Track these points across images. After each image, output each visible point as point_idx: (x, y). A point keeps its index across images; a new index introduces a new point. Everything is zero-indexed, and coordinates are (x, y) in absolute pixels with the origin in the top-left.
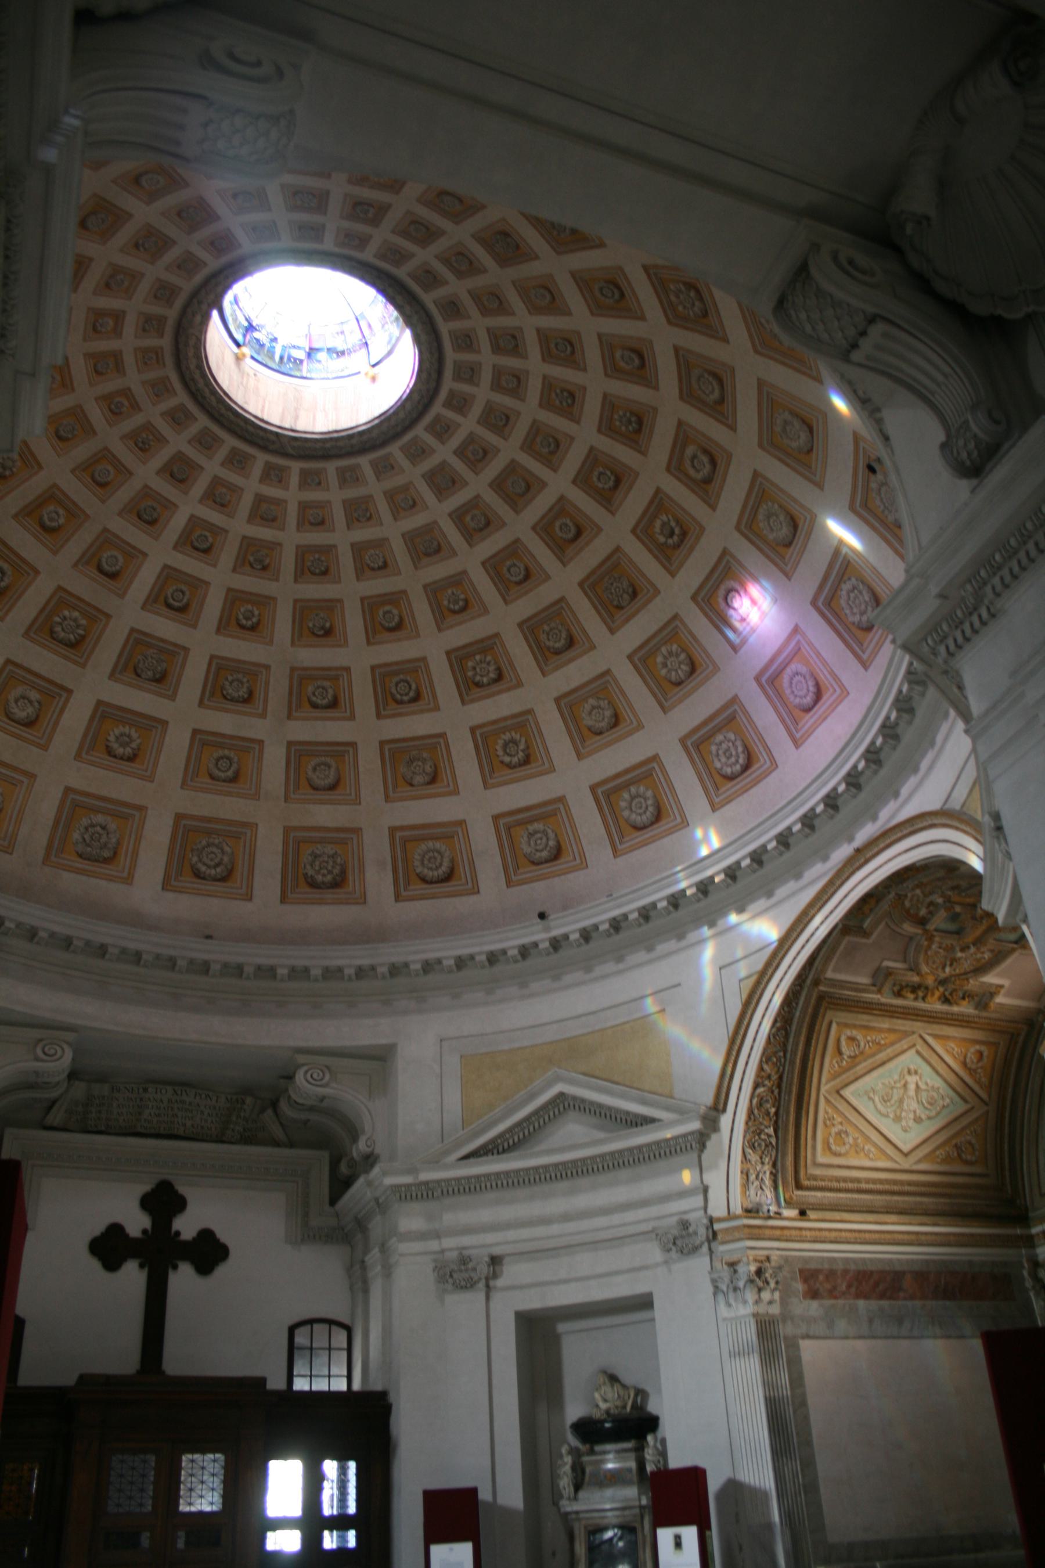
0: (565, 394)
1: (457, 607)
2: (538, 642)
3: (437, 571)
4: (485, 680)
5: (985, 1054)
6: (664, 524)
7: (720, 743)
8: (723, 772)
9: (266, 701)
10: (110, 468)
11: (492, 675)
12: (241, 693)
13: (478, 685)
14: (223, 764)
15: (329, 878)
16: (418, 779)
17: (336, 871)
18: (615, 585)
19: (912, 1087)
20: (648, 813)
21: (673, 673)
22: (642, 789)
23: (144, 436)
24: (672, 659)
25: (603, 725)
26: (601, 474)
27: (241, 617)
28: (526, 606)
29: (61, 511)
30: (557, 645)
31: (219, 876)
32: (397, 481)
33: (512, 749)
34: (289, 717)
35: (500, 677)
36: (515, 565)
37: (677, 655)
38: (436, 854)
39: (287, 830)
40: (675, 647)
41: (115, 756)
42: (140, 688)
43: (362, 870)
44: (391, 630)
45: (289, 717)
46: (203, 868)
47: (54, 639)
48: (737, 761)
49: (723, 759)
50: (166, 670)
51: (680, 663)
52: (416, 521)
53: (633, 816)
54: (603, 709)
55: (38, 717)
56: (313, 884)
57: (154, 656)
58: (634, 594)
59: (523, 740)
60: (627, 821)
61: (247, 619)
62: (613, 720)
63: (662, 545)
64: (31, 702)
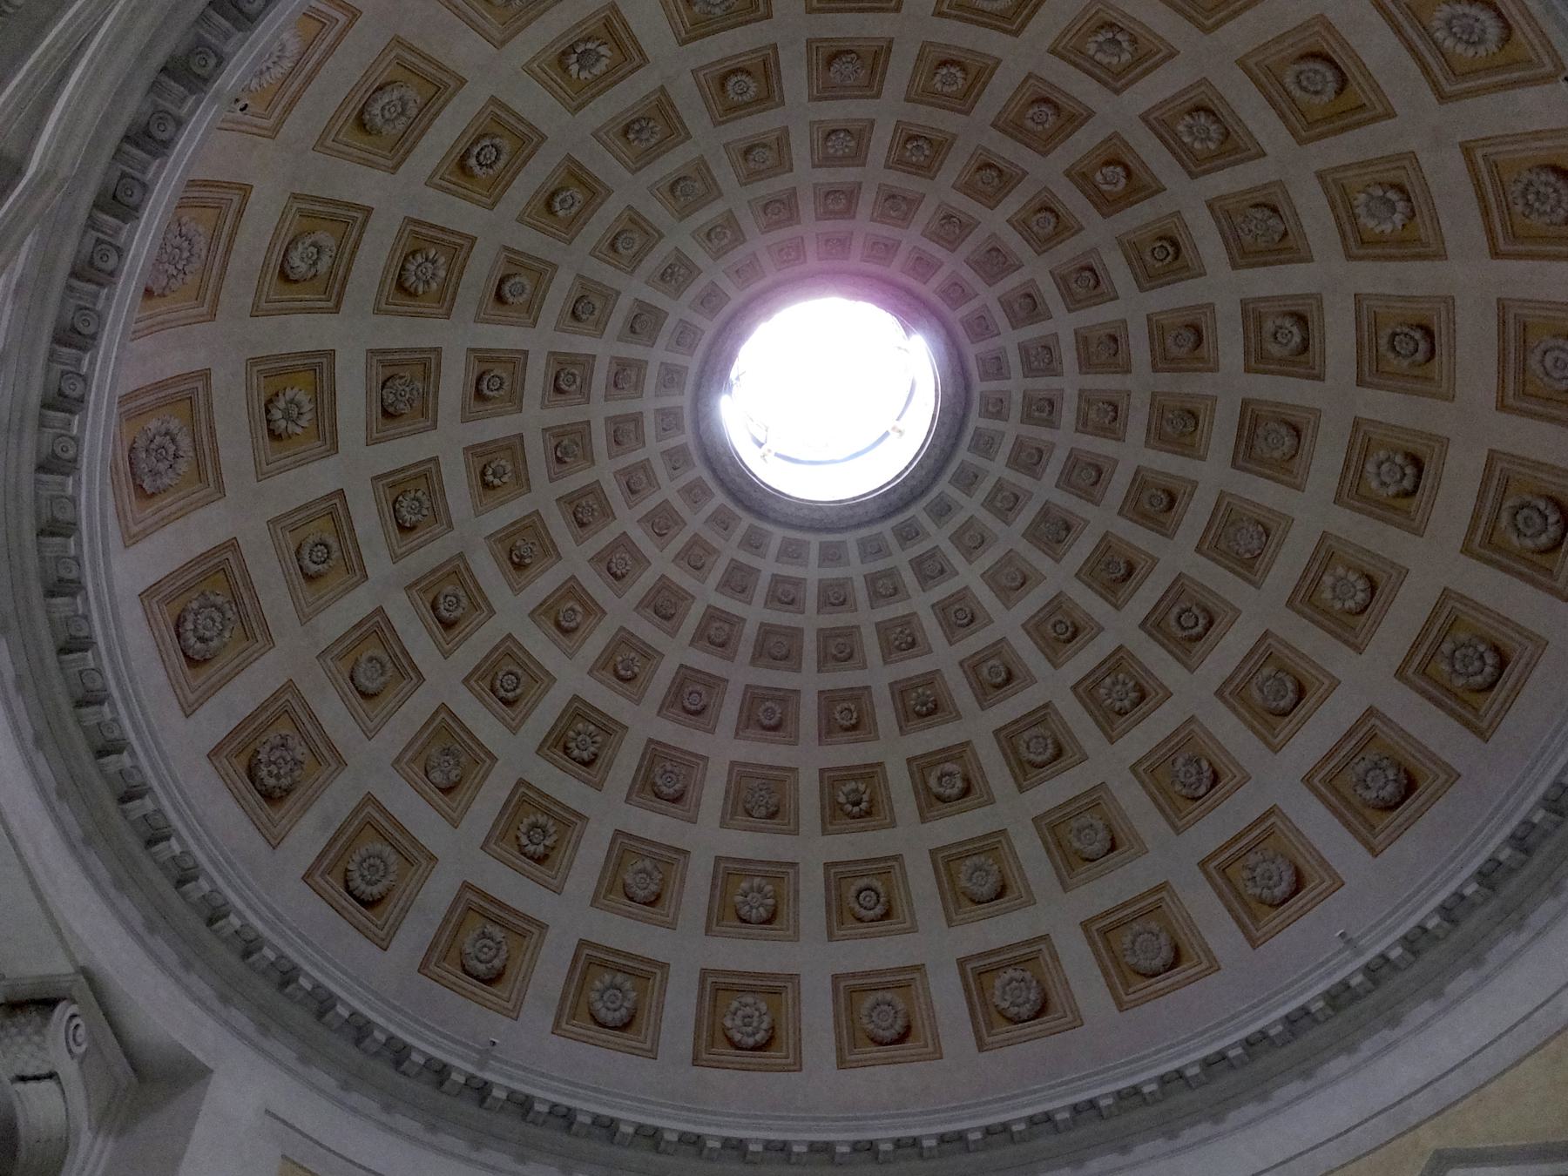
0: (909, 639)
1: (623, 673)
2: (650, 769)
3: (647, 631)
4: (576, 752)
6: (856, 790)
7: (746, 1005)
8: (730, 1033)
9: (411, 551)
10: (636, 248)
11: (586, 756)
12: (408, 517)
13: (566, 750)
14: (320, 552)
15: (272, 782)
16: (437, 776)
17: (285, 782)
18: (763, 792)
20: (617, 1014)
21: (747, 908)
22: (628, 985)
23: (682, 271)
24: (759, 896)
25: (641, 894)
26: (850, 710)
27: (493, 466)
28: (671, 733)
29: (574, 210)
30: (664, 788)
31: (190, 653)
32: (715, 540)
33: (537, 837)
34: (408, 588)
35: (587, 764)
36: (700, 695)
37: (765, 897)
38: (382, 867)
39: (290, 685)
40: (769, 888)
41: (268, 411)
42: (368, 393)
43: (305, 809)
44: (558, 625)
45: (408, 588)
46: (190, 626)
47: (405, 259)
48: (754, 1034)
49: (738, 1022)
50: (402, 414)
51: (761, 905)
52: (683, 579)
53: (599, 1005)
54: (651, 879)
55: (296, 281)
56: (252, 773)
57: (415, 392)
58: (772, 815)
59: (554, 837)
60: (590, 1004)
61: (494, 474)
62: (653, 898)
63: (839, 803)
64: (315, 263)
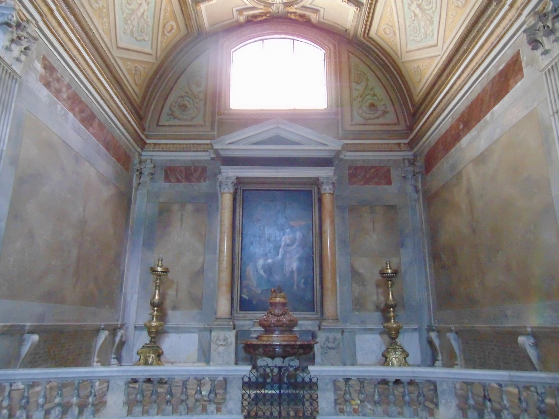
5: (174, 31)
19: (142, 10)
